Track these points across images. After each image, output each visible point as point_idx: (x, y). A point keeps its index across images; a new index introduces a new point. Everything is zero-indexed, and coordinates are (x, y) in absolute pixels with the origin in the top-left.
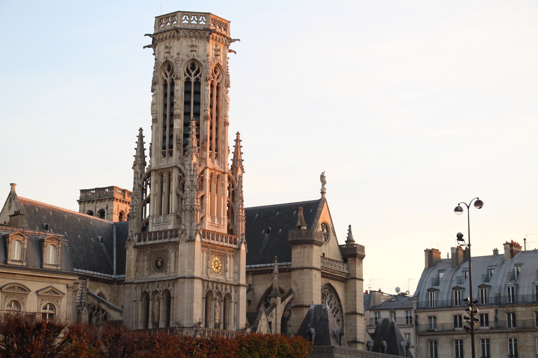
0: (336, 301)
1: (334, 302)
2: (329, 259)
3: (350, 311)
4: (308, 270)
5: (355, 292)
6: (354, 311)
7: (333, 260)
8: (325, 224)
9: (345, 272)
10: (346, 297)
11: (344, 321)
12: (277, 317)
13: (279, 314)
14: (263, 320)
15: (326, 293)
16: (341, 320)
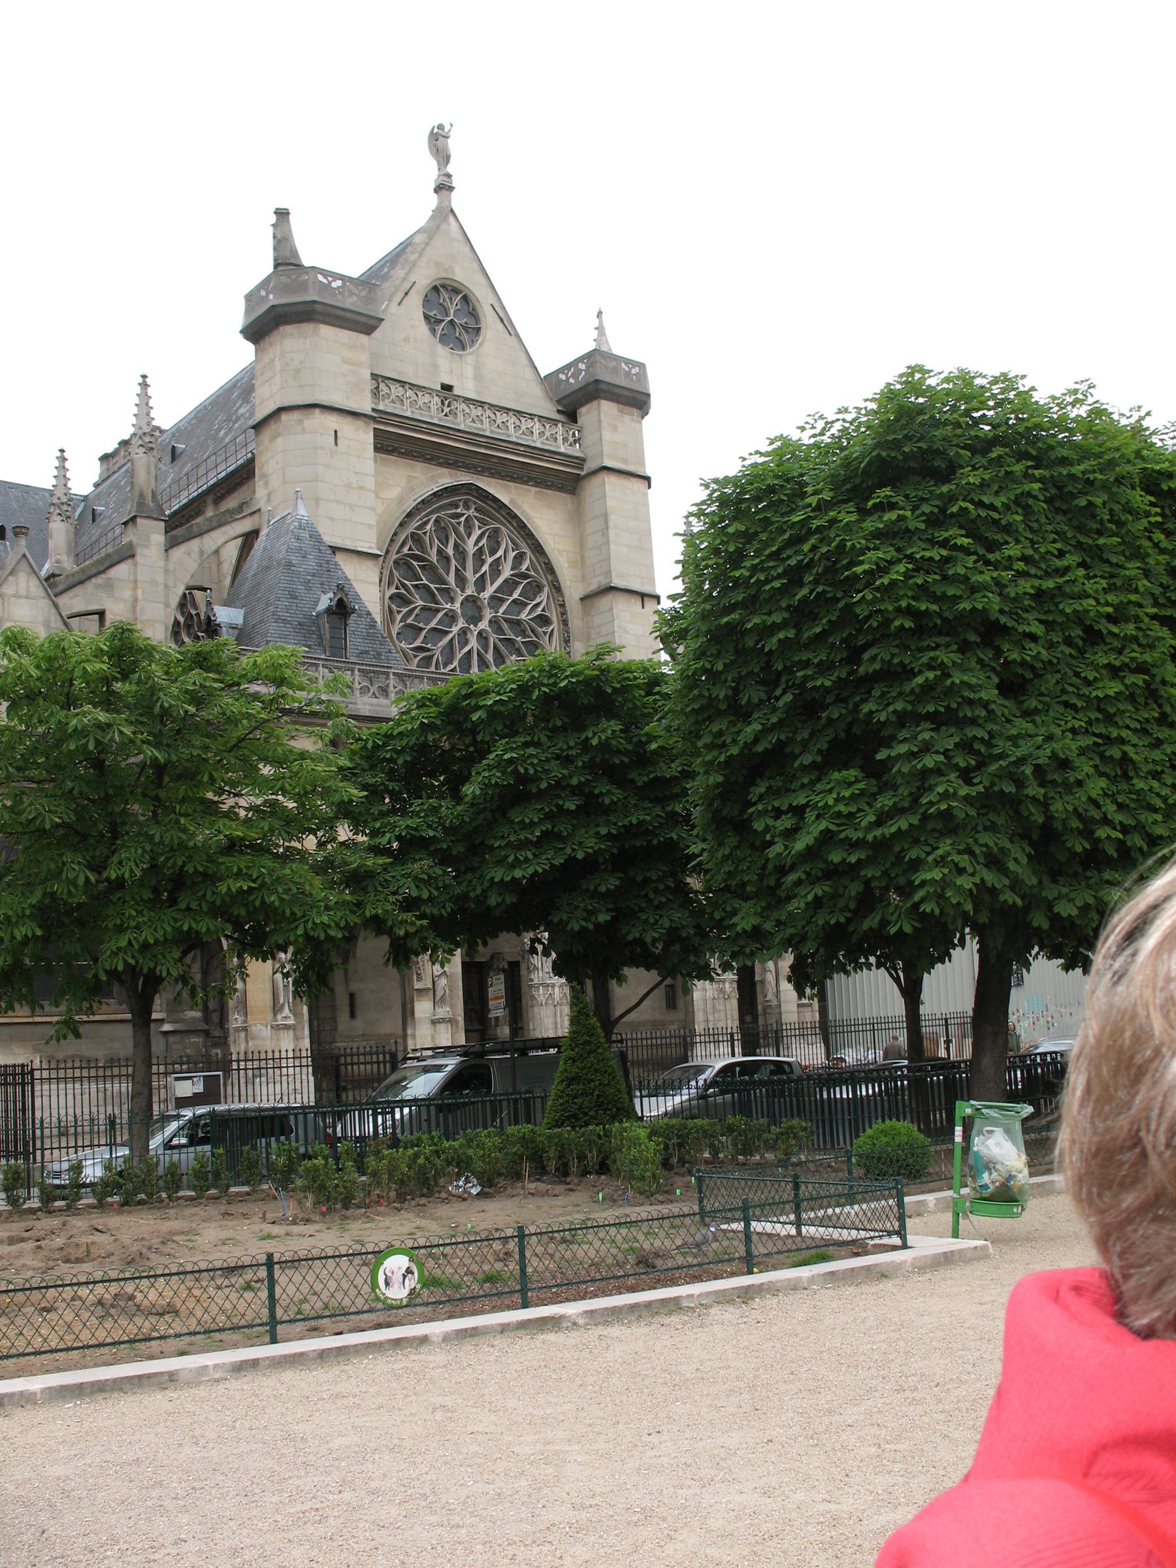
0: (526, 550)
1: (512, 555)
2: (467, 400)
3: (594, 586)
4: (295, 415)
5: (605, 516)
6: (604, 582)
7: (481, 404)
8: (456, 291)
9: (562, 450)
10: (581, 543)
11: (575, 622)
12: (140, 592)
13: (153, 582)
14: (17, 596)
15: (463, 519)
16: (554, 619)
